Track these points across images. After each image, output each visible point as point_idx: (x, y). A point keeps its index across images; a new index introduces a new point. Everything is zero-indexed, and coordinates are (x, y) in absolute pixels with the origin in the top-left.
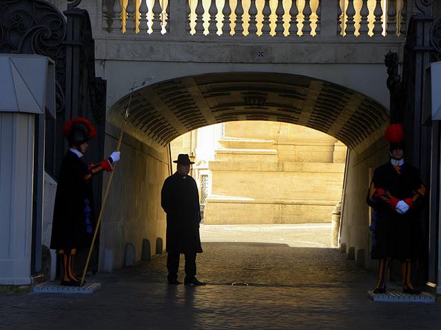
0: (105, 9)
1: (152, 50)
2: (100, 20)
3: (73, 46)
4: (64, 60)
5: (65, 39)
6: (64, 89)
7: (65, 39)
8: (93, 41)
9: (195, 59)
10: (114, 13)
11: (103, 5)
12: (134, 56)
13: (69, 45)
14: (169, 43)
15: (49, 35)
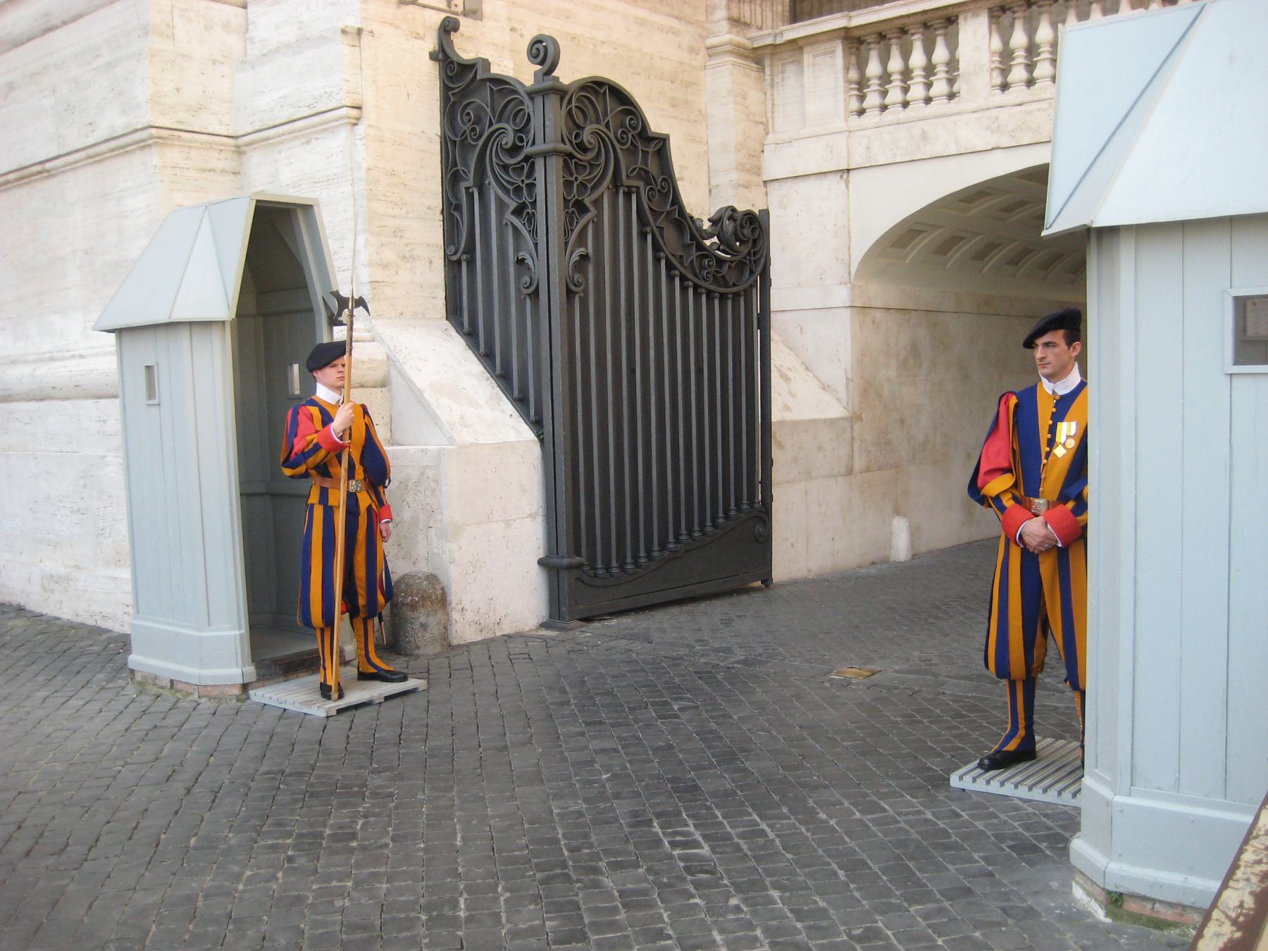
0: (853, 75)
1: (924, 136)
2: (841, 97)
3: (545, 155)
4: (531, 187)
5: (534, 143)
6: (536, 245)
7: (534, 143)
8: (662, 142)
9: (1004, 142)
10: (869, 80)
11: (847, 69)
12: (894, 154)
13: (539, 154)
14: (957, 117)
15: (509, 139)
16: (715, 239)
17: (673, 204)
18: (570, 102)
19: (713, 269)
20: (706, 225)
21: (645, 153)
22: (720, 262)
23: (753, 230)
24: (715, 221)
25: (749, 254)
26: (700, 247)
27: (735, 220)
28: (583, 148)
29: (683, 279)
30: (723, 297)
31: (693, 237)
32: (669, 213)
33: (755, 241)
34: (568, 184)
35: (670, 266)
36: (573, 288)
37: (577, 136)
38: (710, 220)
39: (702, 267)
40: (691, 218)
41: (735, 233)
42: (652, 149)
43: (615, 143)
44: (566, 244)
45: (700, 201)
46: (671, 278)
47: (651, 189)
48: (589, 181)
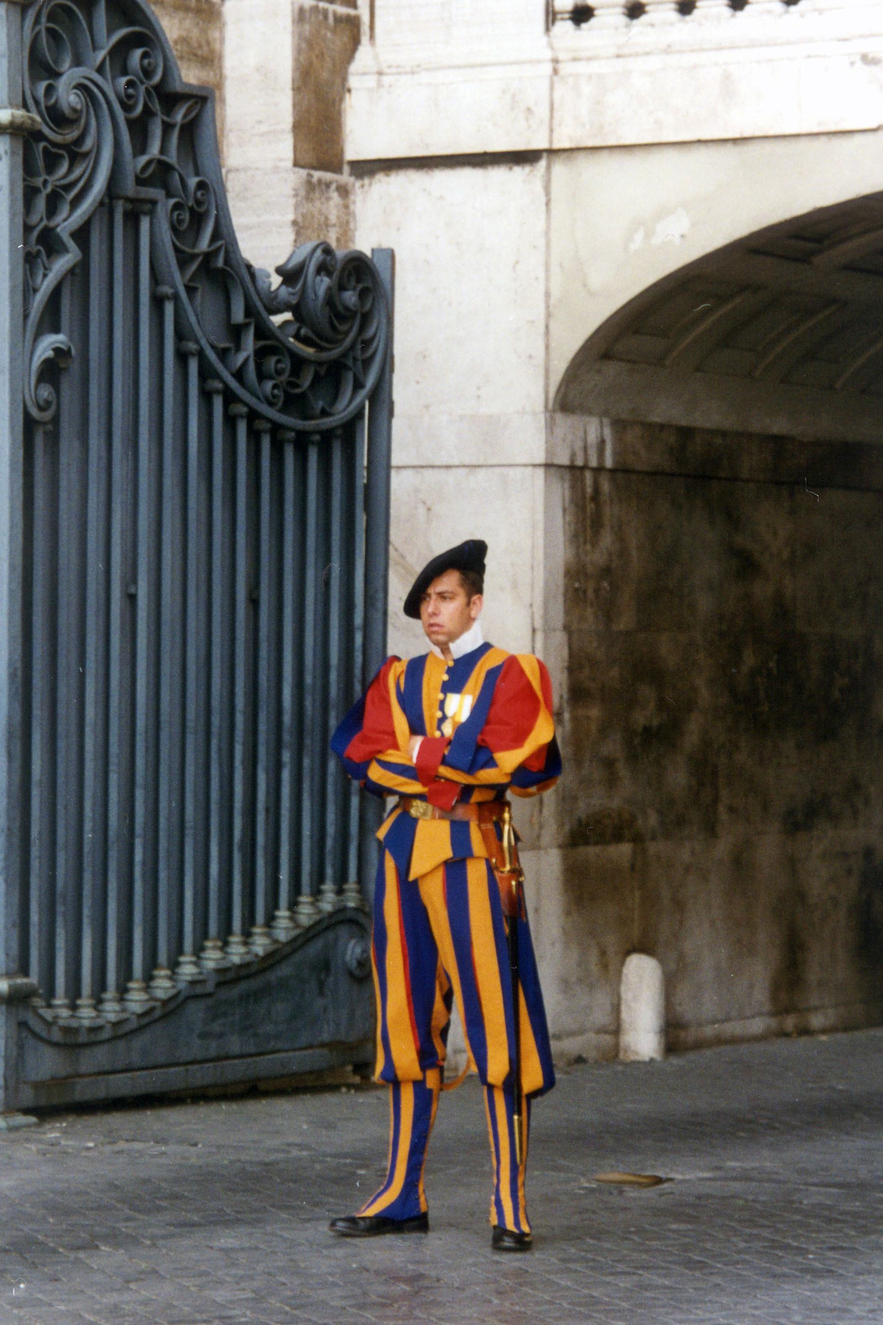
16: (288, 316)
17: (216, 236)
18: (37, 21)
19: (284, 378)
20: (276, 281)
21: (167, 128)
22: (298, 363)
23: (363, 294)
24: (291, 275)
25: (352, 347)
26: (263, 332)
27: (329, 274)
28: (58, 117)
29: (230, 398)
30: (302, 442)
31: (250, 311)
32: (209, 257)
33: (366, 319)
34: (30, 194)
35: (206, 373)
36: (34, 412)
37: (50, 90)
38: (279, 271)
39: (262, 376)
40: (249, 267)
41: (330, 301)
42: (179, 116)
43: (117, 107)
44: (26, 316)
45: (266, 234)
46: (206, 396)
47: (177, 206)
48: (68, 187)
